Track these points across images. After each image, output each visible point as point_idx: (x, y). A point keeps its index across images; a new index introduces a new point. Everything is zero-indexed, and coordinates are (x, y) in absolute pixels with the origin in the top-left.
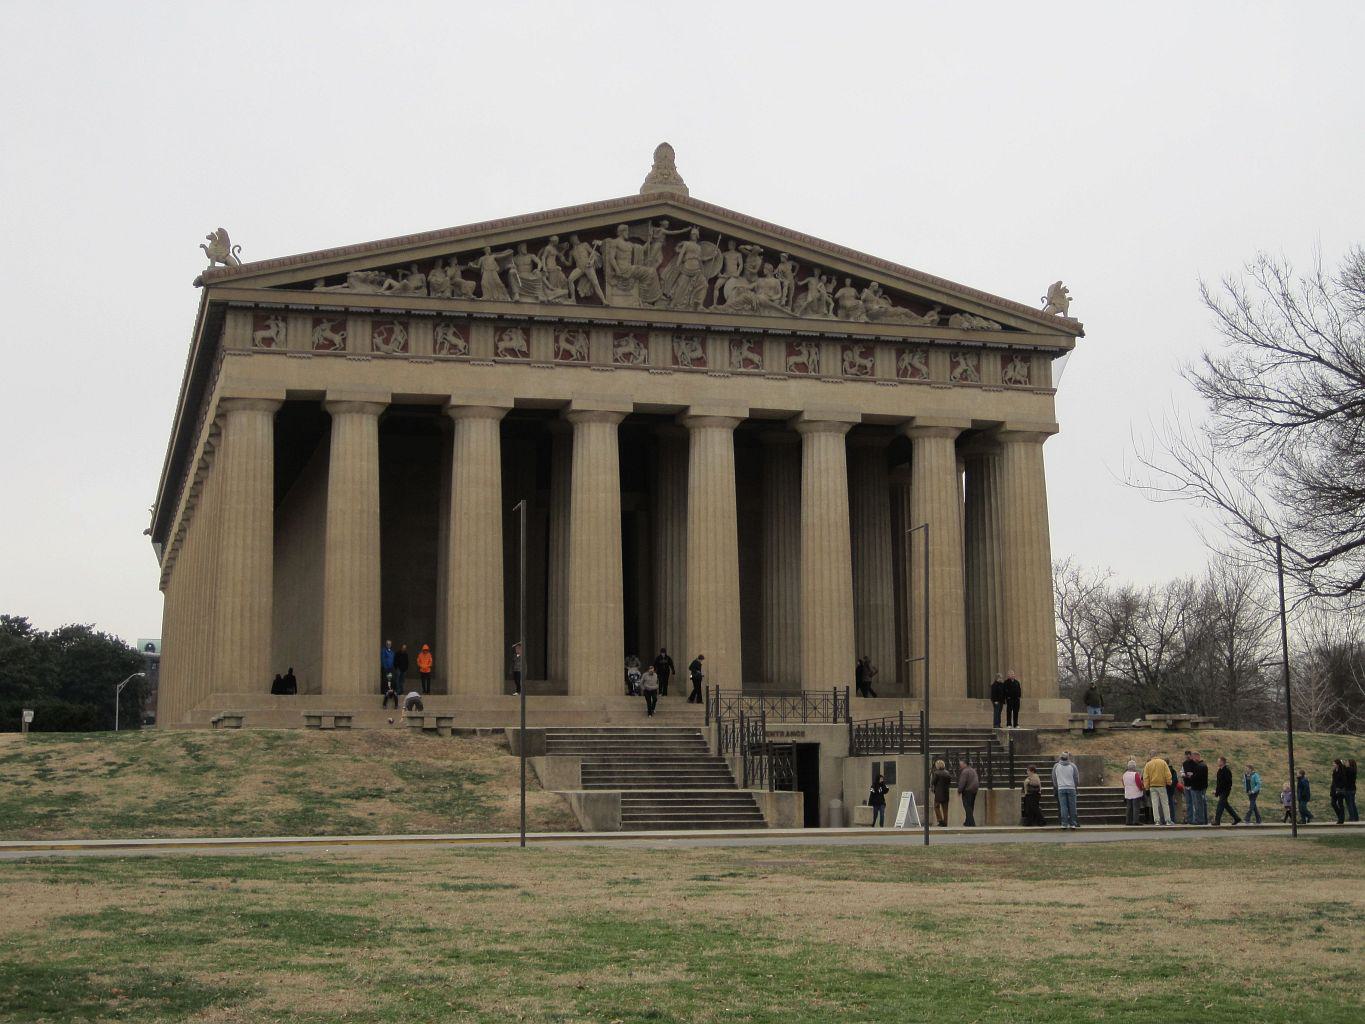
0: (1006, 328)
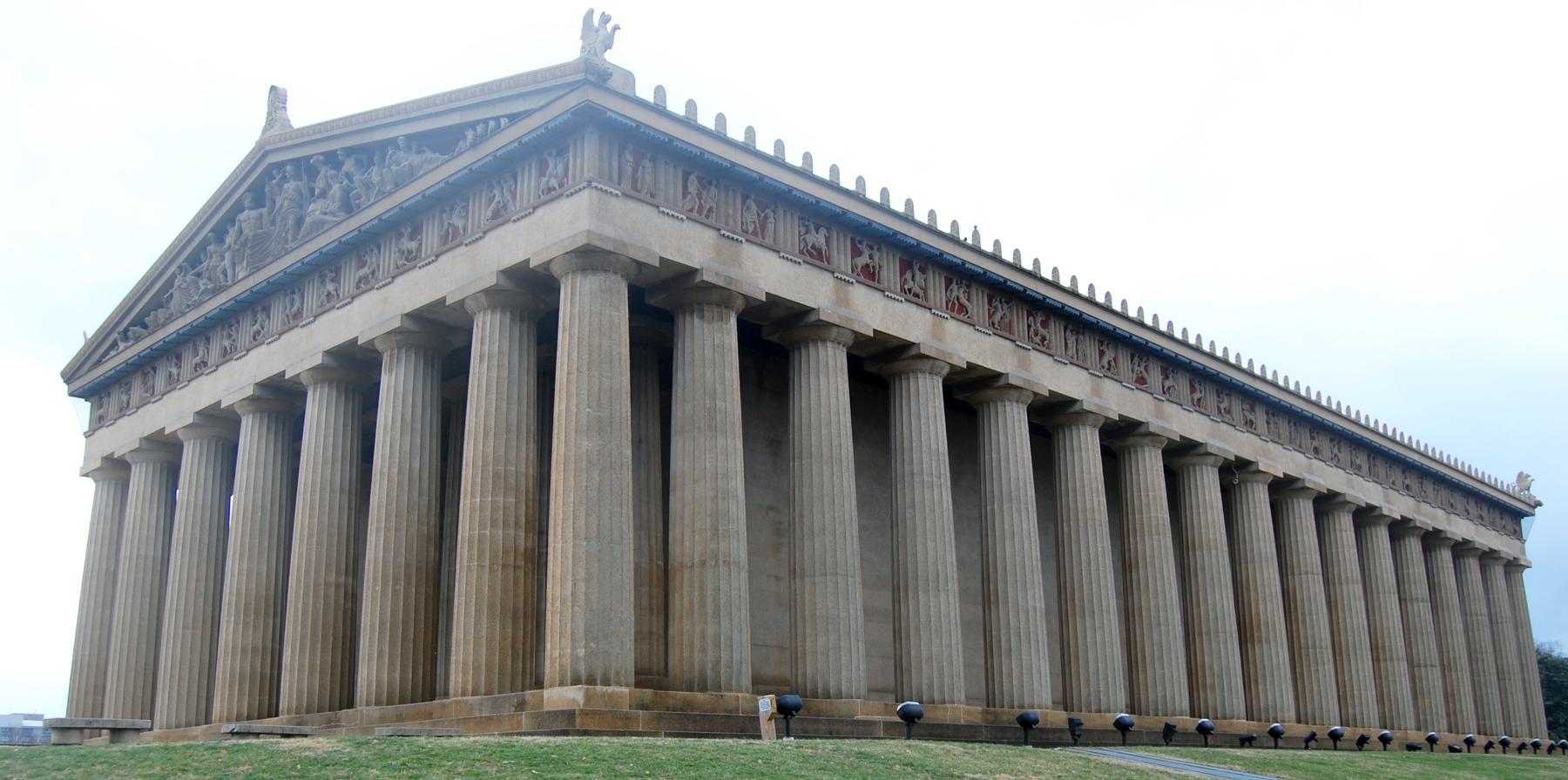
0: (514, 118)
